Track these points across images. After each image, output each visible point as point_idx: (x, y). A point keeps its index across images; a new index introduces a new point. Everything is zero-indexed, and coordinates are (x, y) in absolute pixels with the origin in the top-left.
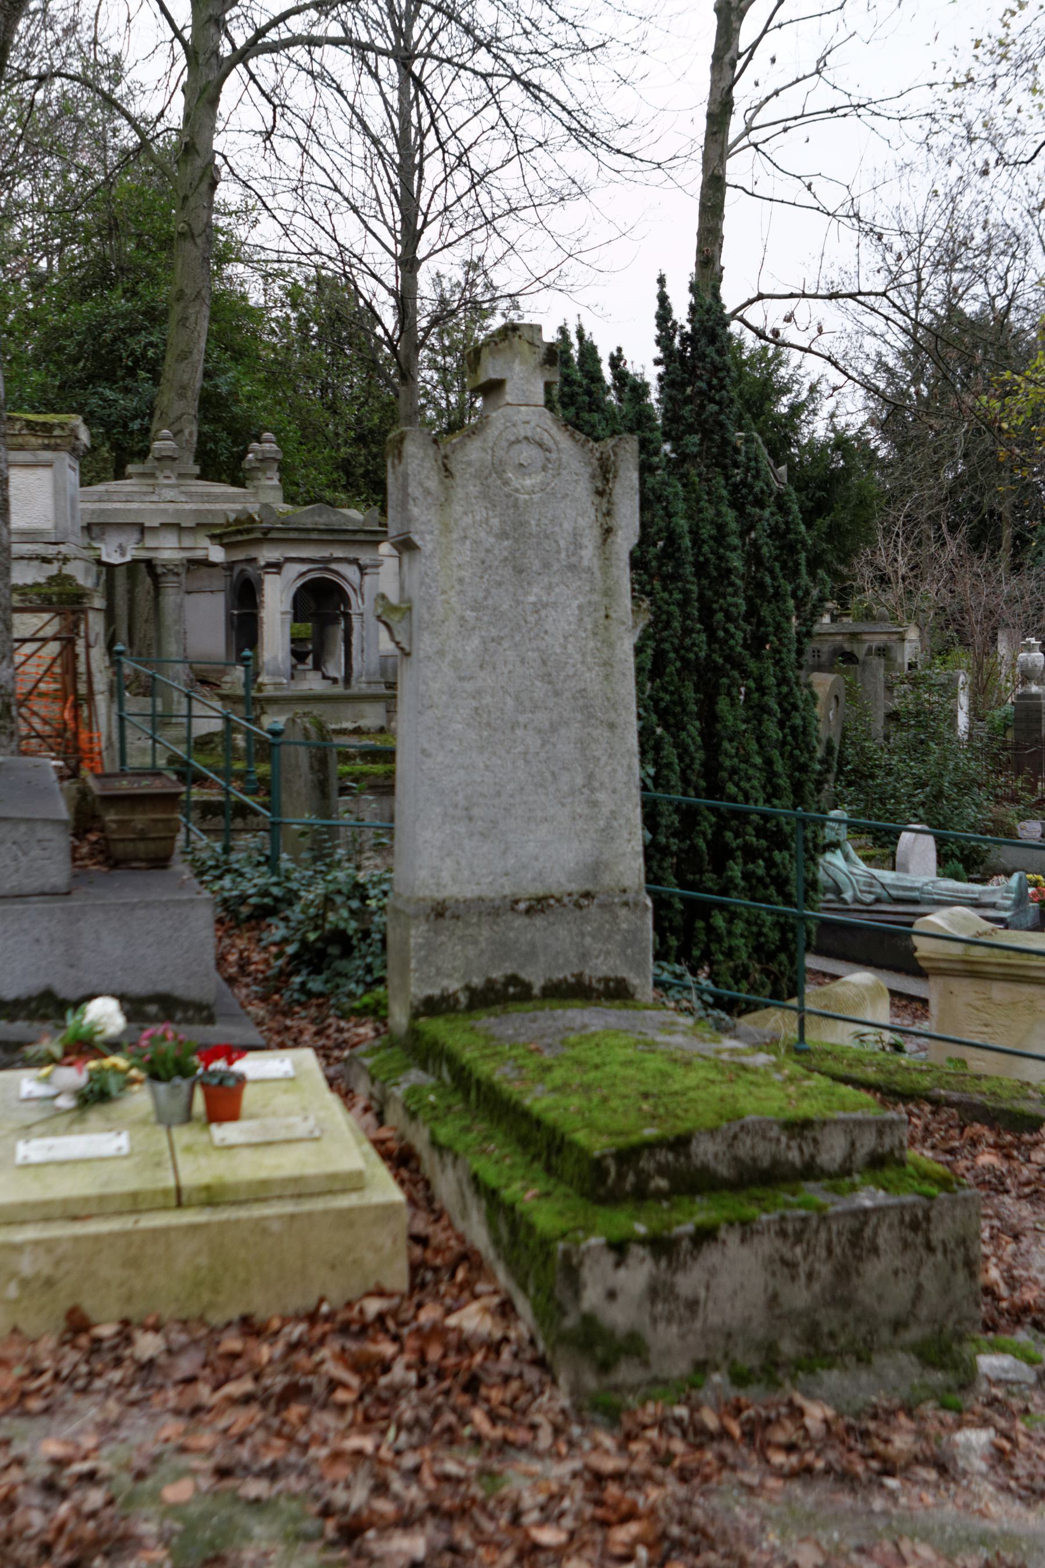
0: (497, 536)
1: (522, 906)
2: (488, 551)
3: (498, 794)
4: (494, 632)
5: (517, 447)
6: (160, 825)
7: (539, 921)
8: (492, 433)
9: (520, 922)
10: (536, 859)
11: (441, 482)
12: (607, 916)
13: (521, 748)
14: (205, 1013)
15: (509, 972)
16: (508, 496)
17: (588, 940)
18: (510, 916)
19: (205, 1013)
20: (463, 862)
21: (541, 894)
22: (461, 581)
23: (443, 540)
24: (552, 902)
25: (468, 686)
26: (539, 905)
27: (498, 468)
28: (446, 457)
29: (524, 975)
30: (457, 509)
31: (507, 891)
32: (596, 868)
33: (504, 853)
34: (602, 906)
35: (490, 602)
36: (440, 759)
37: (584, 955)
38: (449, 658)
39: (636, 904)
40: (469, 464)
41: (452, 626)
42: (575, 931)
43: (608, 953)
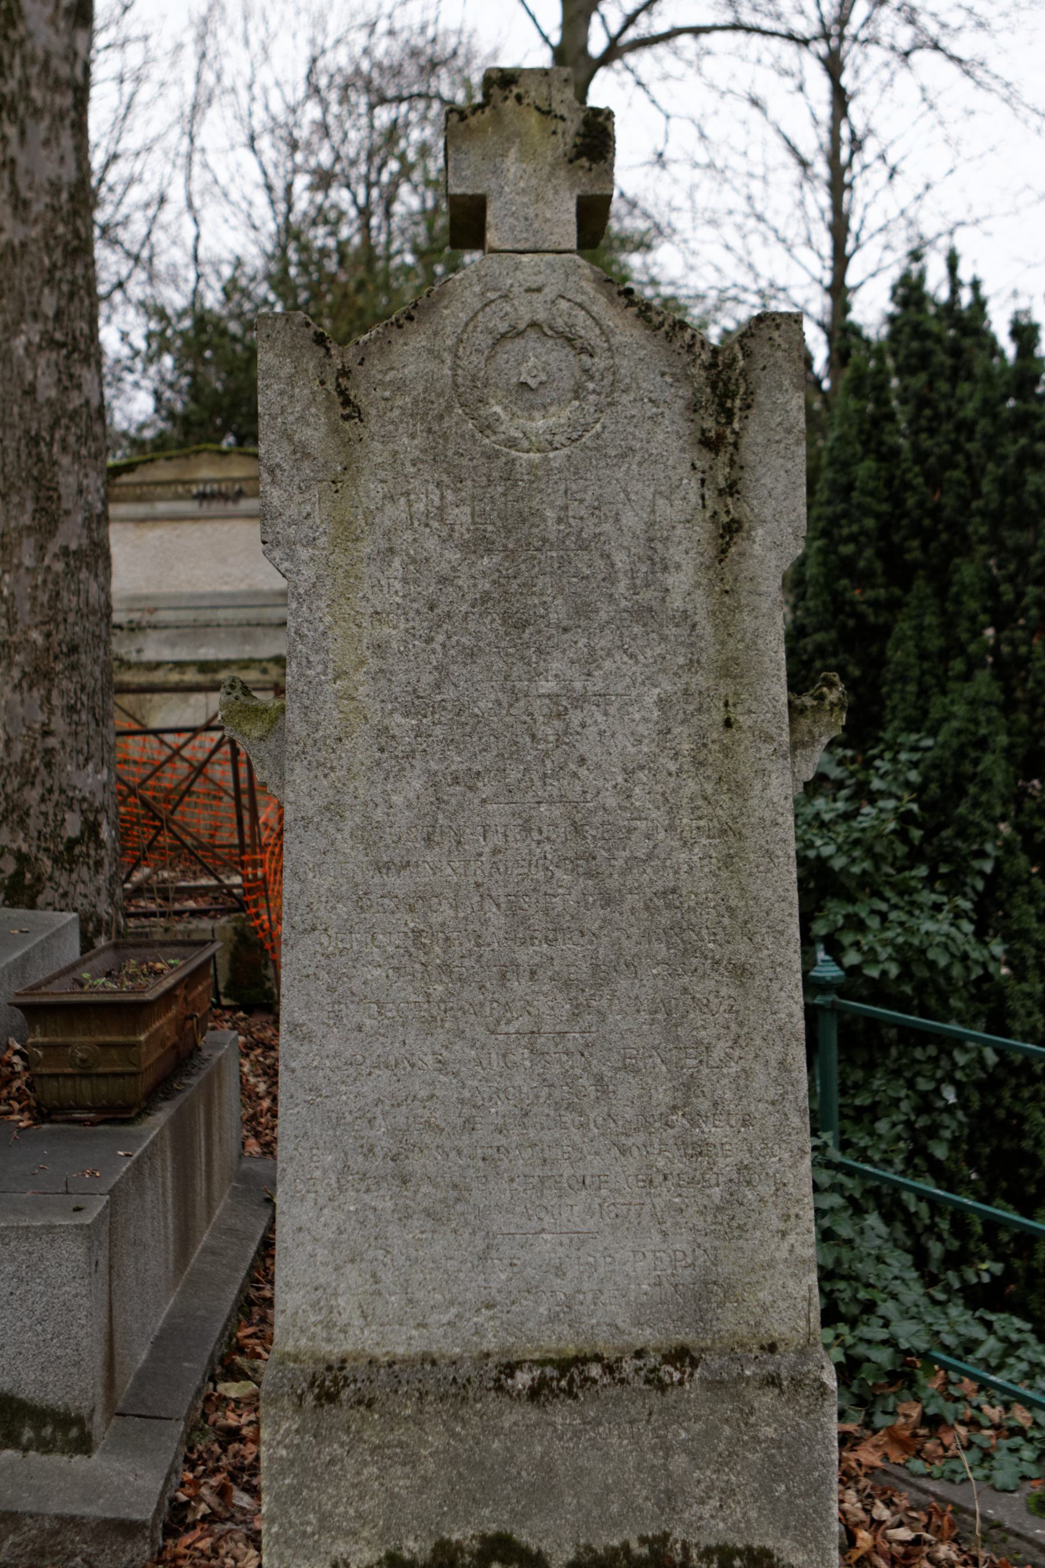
0: (463, 546)
1: (523, 1379)
2: (443, 580)
3: (469, 1125)
4: (458, 762)
5: (514, 346)
6: (114, 1053)
7: (561, 1415)
8: (452, 316)
9: (516, 1416)
10: (560, 1271)
11: (335, 431)
12: (727, 1408)
13: (524, 1023)
14: (74, 1432)
15: (492, 1529)
16: (491, 456)
17: (680, 1461)
18: (493, 1402)
19: (74, 1432)
20: (387, 1277)
21: (571, 1351)
22: (379, 648)
23: (338, 558)
24: (595, 1370)
25: (398, 883)
26: (565, 1377)
27: (469, 394)
28: (344, 373)
29: (523, 1537)
30: (371, 489)
31: (490, 1343)
32: (705, 1293)
33: (483, 1258)
34: (715, 1385)
35: (449, 693)
36: (332, 1046)
37: (670, 1495)
38: (353, 820)
39: (797, 1383)
40: (400, 387)
41: (360, 749)
42: (648, 1440)
43: (729, 1492)
